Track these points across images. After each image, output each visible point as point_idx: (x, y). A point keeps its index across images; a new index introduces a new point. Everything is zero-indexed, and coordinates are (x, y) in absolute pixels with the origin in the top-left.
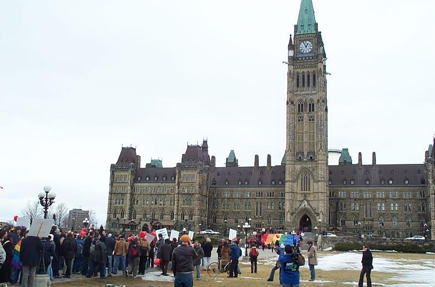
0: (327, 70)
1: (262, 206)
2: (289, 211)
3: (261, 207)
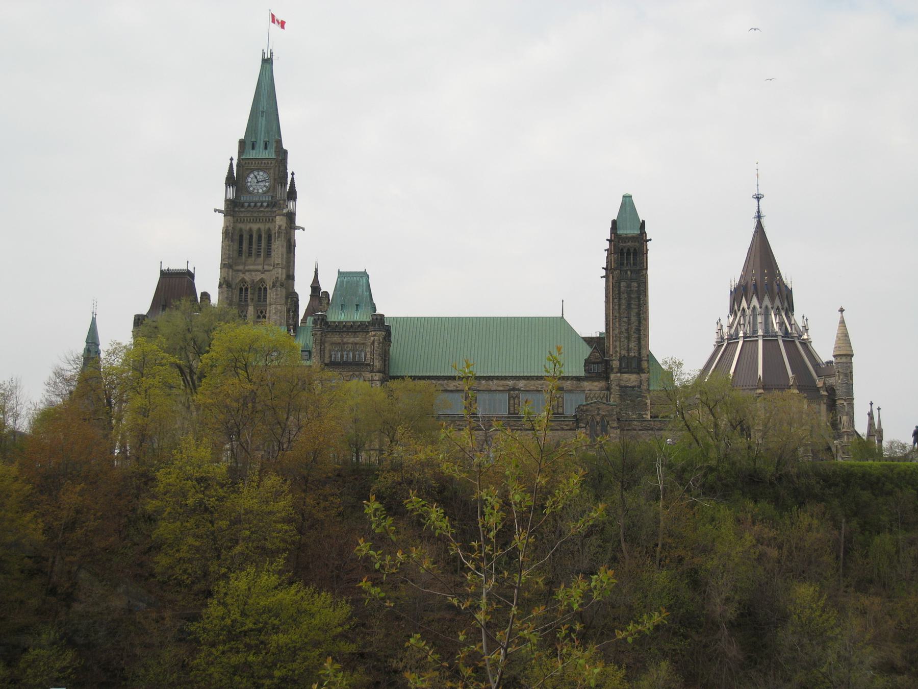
0: (298, 223)
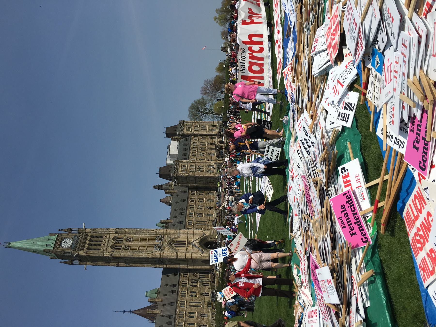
1: (193, 301)
3: (194, 303)
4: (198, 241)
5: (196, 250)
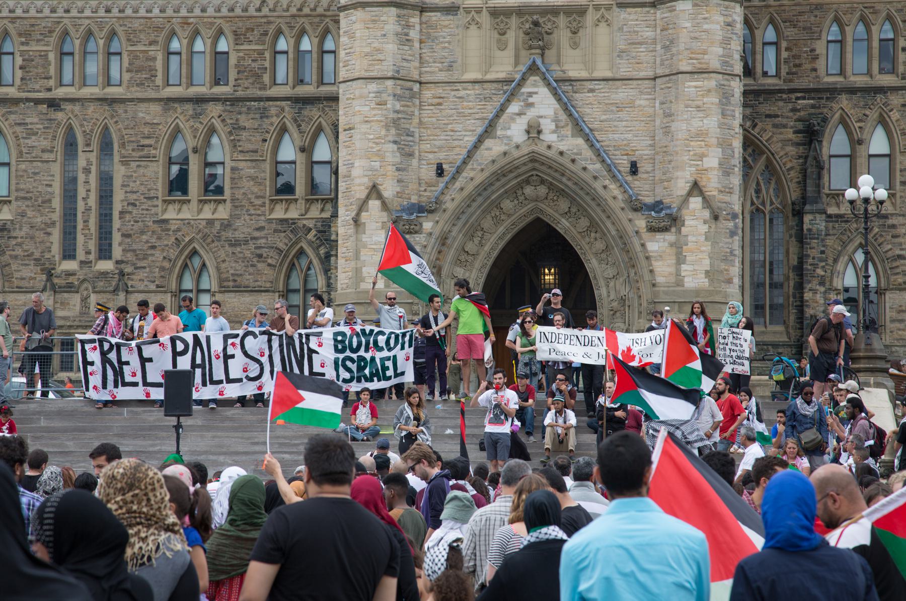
1: (119, 172)
2: (374, 191)
3: (106, 181)
4: (560, 141)
5: (451, 128)
